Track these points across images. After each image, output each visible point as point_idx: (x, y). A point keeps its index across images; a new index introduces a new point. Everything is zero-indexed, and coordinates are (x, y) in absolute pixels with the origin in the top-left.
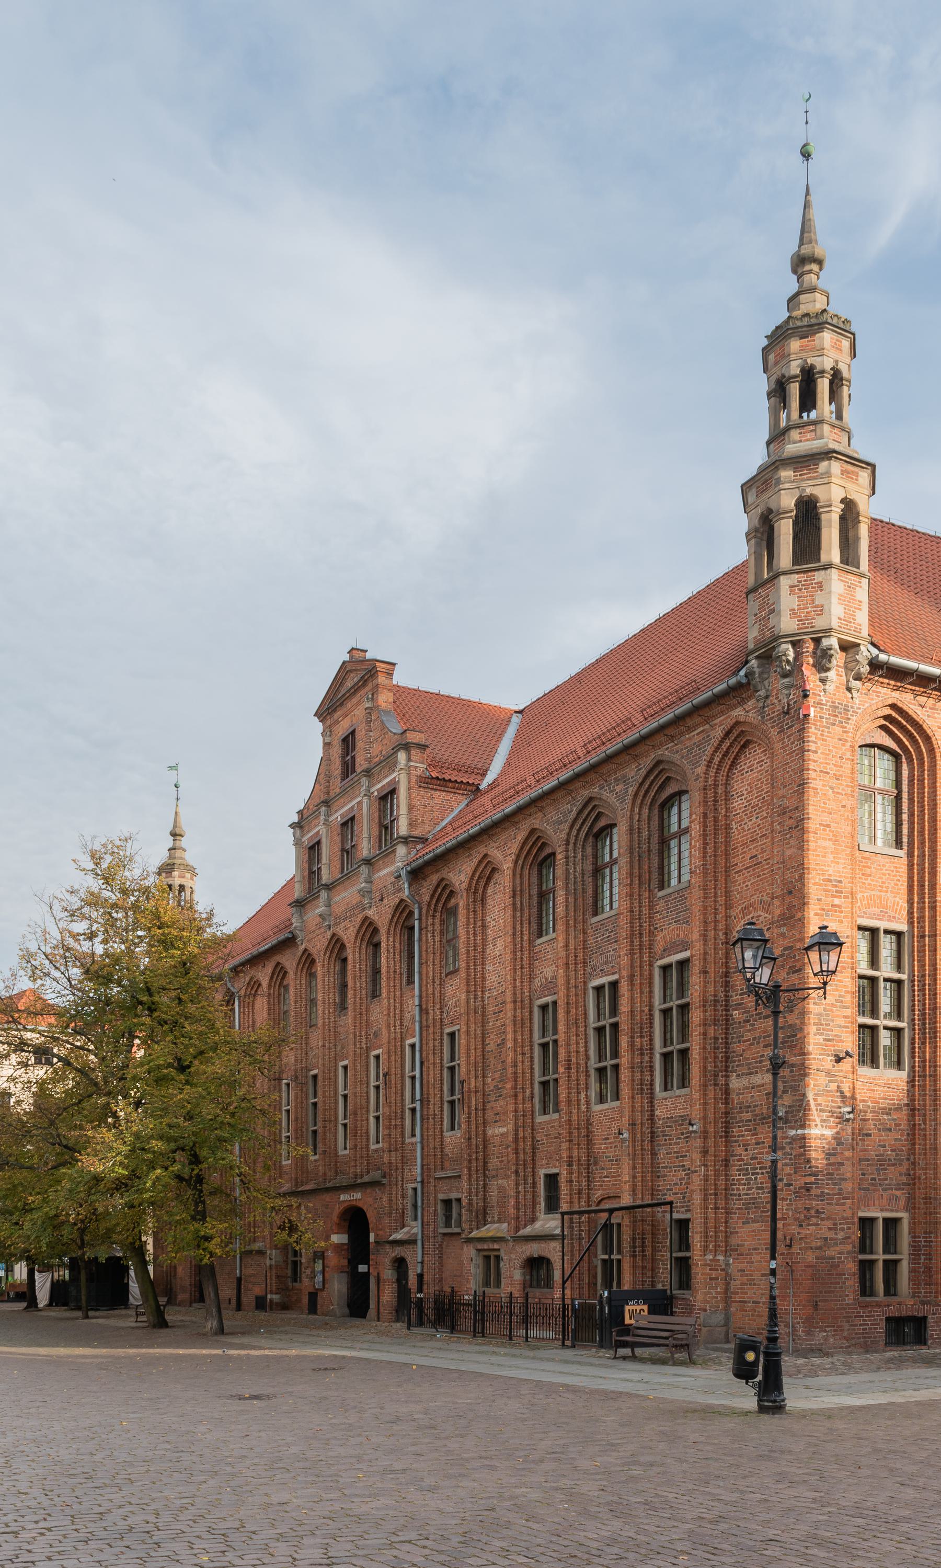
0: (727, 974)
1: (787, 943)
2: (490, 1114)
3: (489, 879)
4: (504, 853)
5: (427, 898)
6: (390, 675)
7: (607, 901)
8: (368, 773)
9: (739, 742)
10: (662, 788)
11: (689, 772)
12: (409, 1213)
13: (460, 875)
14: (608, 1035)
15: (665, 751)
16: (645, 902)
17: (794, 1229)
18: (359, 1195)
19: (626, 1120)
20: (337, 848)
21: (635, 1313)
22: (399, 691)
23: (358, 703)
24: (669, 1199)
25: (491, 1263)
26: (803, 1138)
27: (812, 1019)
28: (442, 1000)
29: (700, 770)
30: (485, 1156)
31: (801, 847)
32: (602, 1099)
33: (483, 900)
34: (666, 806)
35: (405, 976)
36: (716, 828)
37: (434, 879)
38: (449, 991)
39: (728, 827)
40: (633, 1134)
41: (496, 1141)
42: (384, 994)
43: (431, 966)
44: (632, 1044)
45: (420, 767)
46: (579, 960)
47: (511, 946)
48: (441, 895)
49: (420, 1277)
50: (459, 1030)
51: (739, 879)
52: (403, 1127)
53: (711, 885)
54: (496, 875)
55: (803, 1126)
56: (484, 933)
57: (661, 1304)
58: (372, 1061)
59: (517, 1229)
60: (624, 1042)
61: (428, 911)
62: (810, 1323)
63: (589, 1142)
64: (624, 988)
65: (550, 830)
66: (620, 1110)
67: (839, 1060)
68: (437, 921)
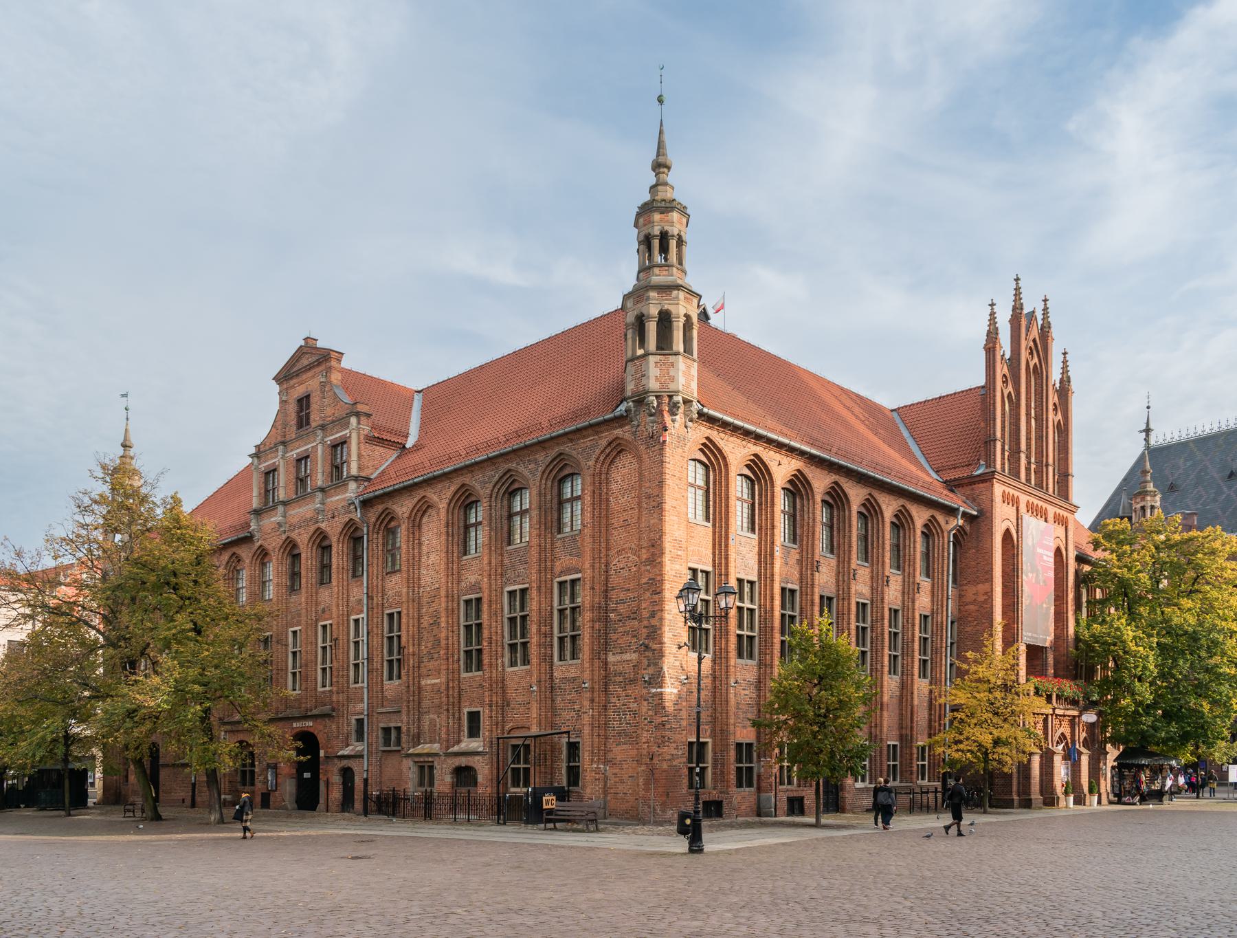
0: (606, 591)
1: (651, 576)
2: (423, 671)
3: (425, 512)
4: (441, 498)
5: (373, 520)
6: (339, 361)
7: (517, 536)
8: (323, 427)
9: (617, 449)
10: (561, 469)
11: (583, 464)
12: (353, 736)
13: (403, 508)
14: (518, 624)
15: (566, 448)
16: (549, 541)
17: (655, 748)
18: (311, 724)
19: (534, 679)
20: (292, 477)
21: (549, 802)
22: (347, 373)
23: (313, 377)
24: (563, 729)
25: (426, 771)
26: (661, 694)
27: (667, 623)
28: (383, 590)
29: (591, 463)
30: (419, 699)
31: (661, 519)
32: (513, 663)
33: (420, 526)
34: (562, 481)
36: (601, 500)
37: (380, 508)
38: (389, 585)
39: (608, 500)
40: (539, 687)
41: (429, 688)
42: (334, 583)
44: (539, 630)
45: (366, 429)
46: (500, 573)
47: (445, 559)
49: (366, 781)
50: (399, 613)
51: (616, 533)
52: (348, 676)
53: (597, 535)
54: (430, 510)
55: (661, 687)
56: (420, 548)
57: (562, 795)
58: (320, 629)
59: (448, 748)
60: (533, 629)
62: (664, 804)
63: (504, 692)
64: (534, 593)
65: (477, 486)
66: (530, 673)
67: (680, 647)
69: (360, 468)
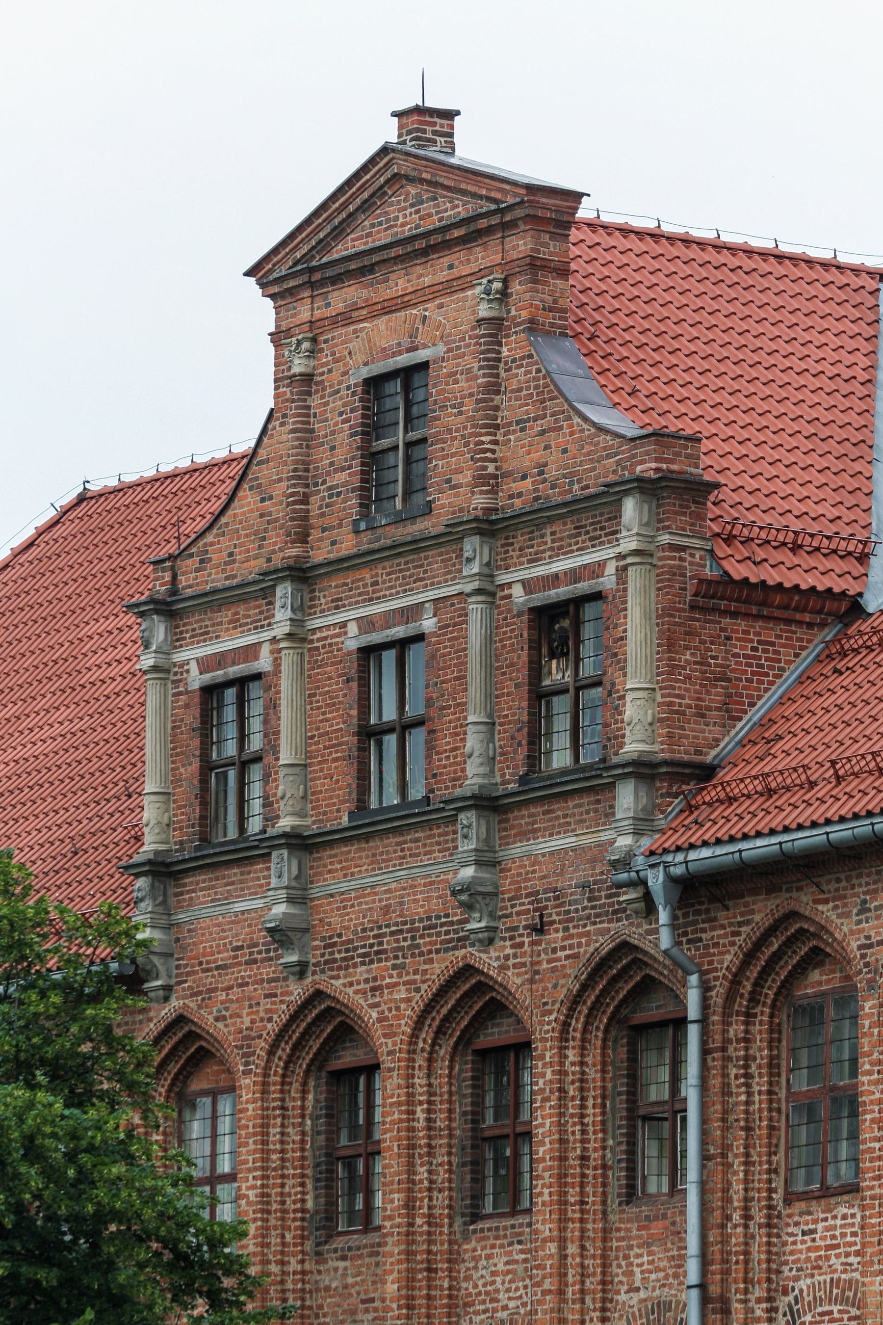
5: (729, 959)
35: (617, 1178)
38: (797, 1244)
43: (737, 1165)
48: (776, 957)
61: (730, 997)
68: (759, 1030)
69: (670, 718)
